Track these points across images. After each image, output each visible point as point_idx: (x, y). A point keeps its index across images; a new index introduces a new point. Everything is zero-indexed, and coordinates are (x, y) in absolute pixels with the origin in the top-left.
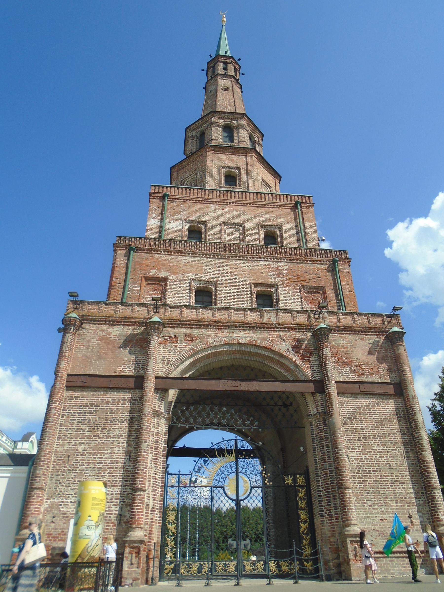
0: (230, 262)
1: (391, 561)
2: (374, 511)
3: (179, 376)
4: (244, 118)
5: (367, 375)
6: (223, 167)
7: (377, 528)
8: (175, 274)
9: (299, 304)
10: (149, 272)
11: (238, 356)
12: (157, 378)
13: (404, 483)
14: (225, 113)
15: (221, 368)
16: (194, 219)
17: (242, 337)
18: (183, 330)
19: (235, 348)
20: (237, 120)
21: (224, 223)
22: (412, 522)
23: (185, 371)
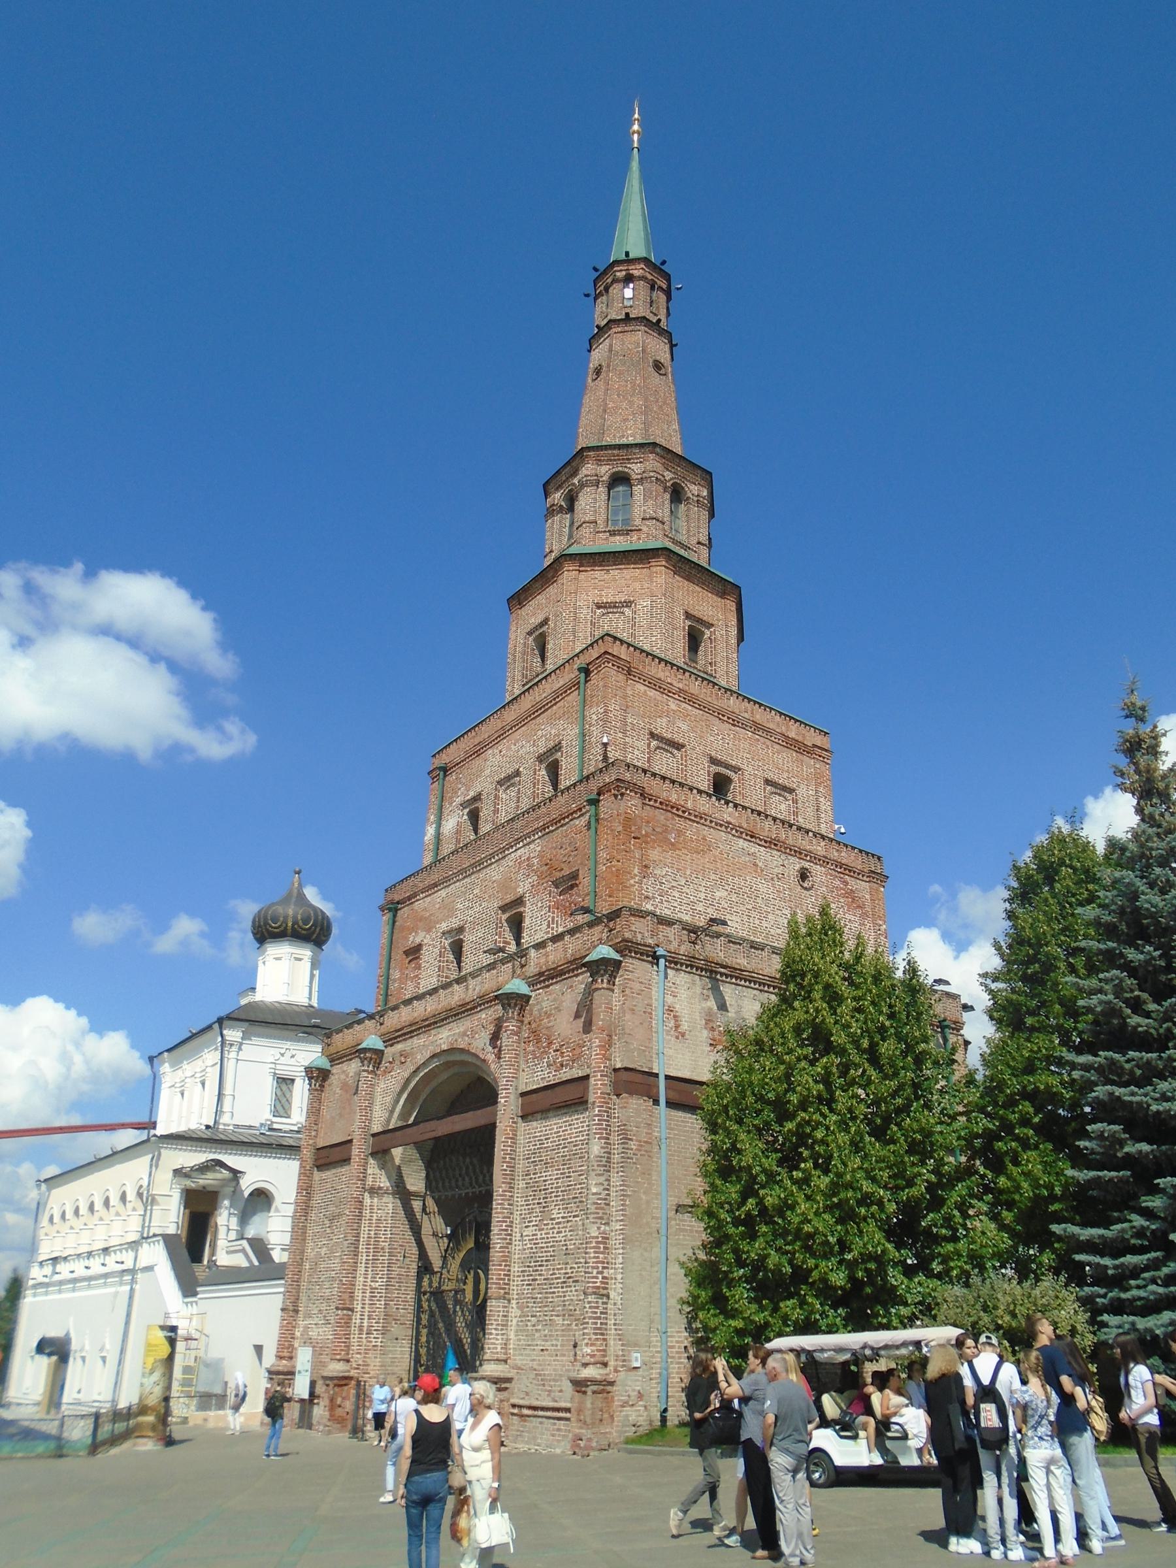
2: (537, 1335)
3: (400, 1124)
4: (587, 456)
6: (530, 633)
7: (535, 1365)
8: (429, 931)
9: (545, 926)
10: (407, 939)
11: (456, 1069)
12: (373, 1135)
13: (577, 1281)
14: (558, 472)
15: (469, 1086)
16: (472, 794)
17: (443, 1038)
18: (399, 1047)
19: (443, 1059)
20: (575, 473)
22: (575, 1355)
23: (404, 1115)
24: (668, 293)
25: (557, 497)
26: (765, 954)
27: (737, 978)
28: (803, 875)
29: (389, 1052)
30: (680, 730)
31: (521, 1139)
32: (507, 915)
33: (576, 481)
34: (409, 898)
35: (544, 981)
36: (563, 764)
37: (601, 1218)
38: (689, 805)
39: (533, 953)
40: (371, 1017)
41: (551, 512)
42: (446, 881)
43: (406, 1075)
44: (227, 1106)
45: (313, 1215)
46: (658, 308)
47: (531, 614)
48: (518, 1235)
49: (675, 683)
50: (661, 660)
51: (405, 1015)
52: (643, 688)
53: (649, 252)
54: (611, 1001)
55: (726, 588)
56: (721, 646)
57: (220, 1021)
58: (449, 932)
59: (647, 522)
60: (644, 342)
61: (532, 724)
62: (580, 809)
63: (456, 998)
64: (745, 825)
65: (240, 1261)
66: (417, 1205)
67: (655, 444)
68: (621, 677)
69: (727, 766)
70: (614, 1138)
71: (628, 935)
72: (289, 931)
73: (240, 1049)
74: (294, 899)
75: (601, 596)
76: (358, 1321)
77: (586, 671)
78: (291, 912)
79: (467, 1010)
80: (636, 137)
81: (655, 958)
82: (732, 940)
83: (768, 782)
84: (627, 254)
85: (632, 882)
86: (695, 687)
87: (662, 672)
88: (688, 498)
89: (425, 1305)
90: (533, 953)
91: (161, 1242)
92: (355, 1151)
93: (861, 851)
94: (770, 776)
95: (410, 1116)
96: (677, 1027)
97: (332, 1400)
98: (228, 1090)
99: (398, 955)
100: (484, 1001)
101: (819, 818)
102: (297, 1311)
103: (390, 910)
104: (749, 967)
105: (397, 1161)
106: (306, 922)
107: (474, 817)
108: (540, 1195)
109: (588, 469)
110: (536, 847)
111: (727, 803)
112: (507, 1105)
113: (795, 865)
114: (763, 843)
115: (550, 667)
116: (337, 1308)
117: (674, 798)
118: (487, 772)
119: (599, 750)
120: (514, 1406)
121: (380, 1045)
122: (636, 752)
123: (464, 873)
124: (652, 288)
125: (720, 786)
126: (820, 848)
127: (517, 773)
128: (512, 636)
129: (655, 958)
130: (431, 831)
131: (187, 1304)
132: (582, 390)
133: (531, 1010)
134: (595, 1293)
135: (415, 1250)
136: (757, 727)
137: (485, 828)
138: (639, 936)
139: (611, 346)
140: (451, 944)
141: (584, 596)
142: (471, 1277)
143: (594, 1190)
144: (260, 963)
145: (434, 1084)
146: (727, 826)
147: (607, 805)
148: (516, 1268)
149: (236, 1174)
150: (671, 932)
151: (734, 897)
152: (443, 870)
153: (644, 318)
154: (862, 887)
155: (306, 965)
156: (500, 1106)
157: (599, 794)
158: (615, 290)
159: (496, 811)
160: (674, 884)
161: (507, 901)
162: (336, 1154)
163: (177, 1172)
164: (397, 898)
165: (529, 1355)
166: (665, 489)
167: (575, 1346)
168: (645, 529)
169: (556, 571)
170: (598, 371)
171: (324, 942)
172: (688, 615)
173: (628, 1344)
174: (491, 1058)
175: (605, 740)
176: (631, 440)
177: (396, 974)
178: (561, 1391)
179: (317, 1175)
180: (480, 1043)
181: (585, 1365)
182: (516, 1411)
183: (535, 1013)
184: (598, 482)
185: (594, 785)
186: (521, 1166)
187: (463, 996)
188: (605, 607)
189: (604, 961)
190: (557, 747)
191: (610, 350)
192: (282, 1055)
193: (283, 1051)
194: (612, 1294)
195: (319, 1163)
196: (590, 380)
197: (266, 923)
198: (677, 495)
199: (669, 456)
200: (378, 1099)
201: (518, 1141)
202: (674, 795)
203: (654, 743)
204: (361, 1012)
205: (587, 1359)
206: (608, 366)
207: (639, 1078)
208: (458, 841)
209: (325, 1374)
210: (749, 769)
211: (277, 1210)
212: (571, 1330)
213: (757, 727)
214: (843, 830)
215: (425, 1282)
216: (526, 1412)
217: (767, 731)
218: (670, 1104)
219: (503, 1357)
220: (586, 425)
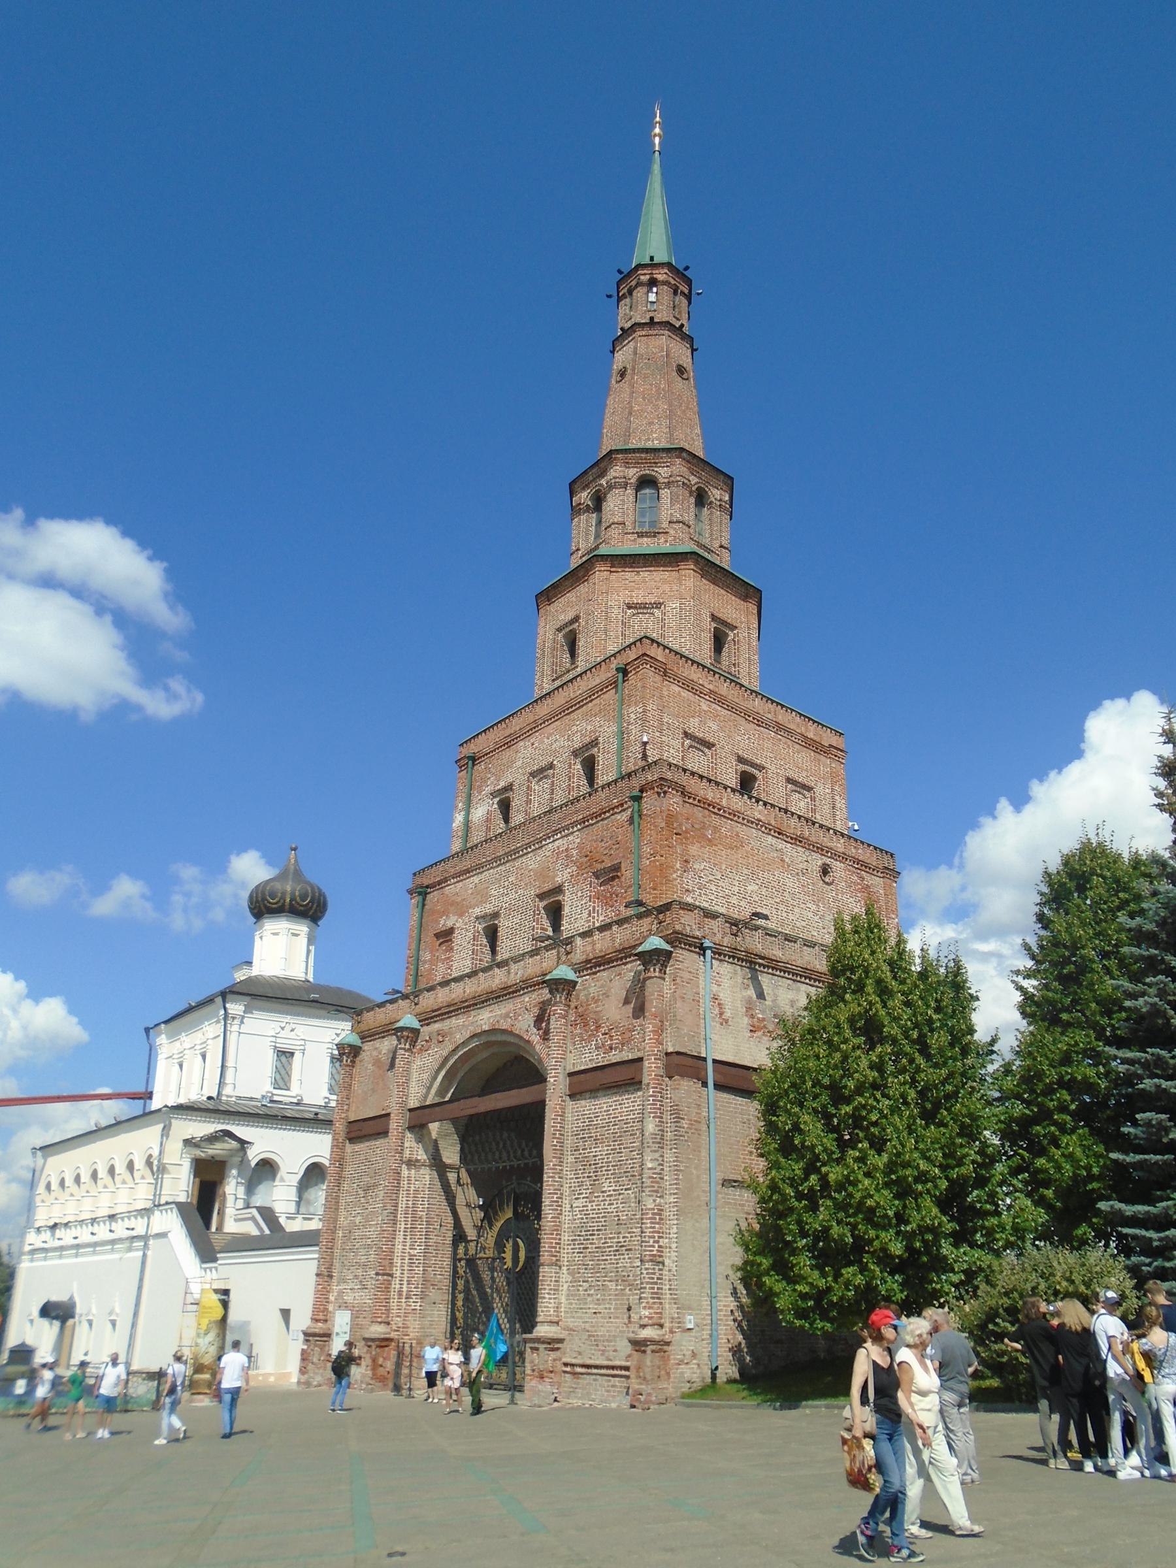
0: (517, 863)
1: (595, 1380)
2: (589, 1299)
5: (616, 1049)
6: (559, 630)
8: (461, 915)
9: (585, 915)
11: (495, 1049)
12: (410, 1110)
14: (585, 472)
16: (502, 784)
17: (484, 1018)
18: (437, 1026)
19: (483, 1039)
20: (602, 474)
21: (531, 774)
23: (442, 1091)
24: (689, 297)
25: (584, 497)
26: (797, 946)
27: (773, 968)
28: (825, 870)
29: (425, 1031)
30: (710, 729)
31: (569, 1116)
32: (545, 903)
33: (603, 482)
34: (439, 883)
35: (591, 968)
36: (600, 759)
37: (657, 1191)
38: (724, 803)
39: (579, 941)
40: (405, 997)
41: (576, 511)
42: (479, 868)
43: (445, 1054)
44: (229, 1078)
45: (345, 1186)
46: (680, 312)
47: (562, 610)
48: (568, 1206)
49: (706, 685)
50: (693, 662)
51: (442, 996)
52: (677, 689)
53: (670, 256)
54: (660, 989)
55: (749, 593)
56: (744, 647)
57: (224, 995)
58: (483, 917)
59: (674, 526)
60: (668, 346)
61: (566, 720)
62: (622, 805)
63: (497, 981)
64: (773, 823)
65: (250, 1229)
66: (452, 1177)
67: (682, 450)
68: (658, 678)
69: (753, 765)
70: (667, 1117)
71: (678, 927)
72: (287, 907)
73: (242, 1022)
74: (291, 877)
75: (632, 597)
76: (398, 1286)
77: (624, 671)
78: (289, 889)
79: (509, 993)
80: (657, 140)
81: (703, 950)
82: (769, 933)
83: (789, 780)
84: (652, 258)
86: (724, 688)
87: (695, 674)
88: (711, 503)
89: (461, 1272)
90: (579, 941)
91: (175, 1210)
92: (393, 1125)
93: (876, 848)
94: (791, 774)
95: (447, 1092)
96: (721, 1014)
97: (374, 1360)
98: (230, 1063)
99: (428, 937)
100: (528, 985)
101: (834, 815)
102: (331, 1277)
103: (420, 893)
104: (784, 959)
105: (434, 1135)
106: (303, 898)
107: (505, 807)
108: (591, 1171)
109: (616, 471)
110: (575, 839)
111: (750, 798)
112: (556, 1085)
113: (818, 860)
115: (582, 665)
116: (377, 1274)
117: (710, 796)
118: (519, 763)
119: (638, 748)
120: (566, 1365)
121: (416, 1024)
122: (672, 751)
123: (498, 860)
124: (675, 293)
125: (746, 783)
126: (839, 845)
127: (551, 766)
128: (541, 631)
129: (703, 950)
130: (459, 818)
131: (205, 1269)
132: (607, 390)
133: (578, 995)
134: (651, 1261)
135: (450, 1220)
136: (779, 728)
137: (517, 818)
138: (688, 928)
139: (635, 348)
140: (484, 929)
141: (615, 596)
142: (509, 1247)
143: (650, 1165)
144: (257, 938)
145: (473, 1061)
146: (757, 823)
147: (650, 802)
148: (565, 1237)
149: (243, 1143)
150: (715, 925)
152: (472, 858)
153: (668, 322)
155: (303, 941)
156: (549, 1086)
157: (641, 791)
158: (639, 293)
159: (529, 802)
160: (711, 878)
161: (545, 889)
162: (369, 1128)
163: (188, 1142)
164: (426, 882)
165: (581, 1318)
166: (691, 492)
167: (629, 1309)
168: (672, 532)
169: (588, 571)
170: (622, 374)
171: (320, 918)
172: (714, 618)
173: (684, 1307)
174: (535, 1037)
175: (645, 739)
176: (656, 444)
177: (426, 956)
178: (615, 1351)
179: (349, 1148)
180: (525, 1025)
181: (643, 1326)
182: (568, 1369)
183: (582, 997)
184: (626, 484)
185: (636, 782)
186: (569, 1142)
187: (504, 979)
188: (636, 608)
189: (657, 952)
190: (594, 743)
191: (635, 353)
192: (283, 1028)
193: (283, 1025)
194: (667, 1262)
195: (353, 1135)
196: (613, 382)
197: (264, 899)
198: (701, 499)
200: (415, 1076)
201: (566, 1119)
202: (710, 794)
203: (688, 742)
204: (398, 992)
205: (645, 1321)
206: (633, 369)
207: (690, 1061)
208: (488, 829)
209: (367, 1336)
210: (772, 768)
211: (282, 1180)
212: (623, 1295)
213: (779, 728)
214: (856, 827)
215: (461, 1250)
216: (579, 1370)
217: (788, 731)
218: (718, 1087)
219: (556, 1319)
220: (611, 426)
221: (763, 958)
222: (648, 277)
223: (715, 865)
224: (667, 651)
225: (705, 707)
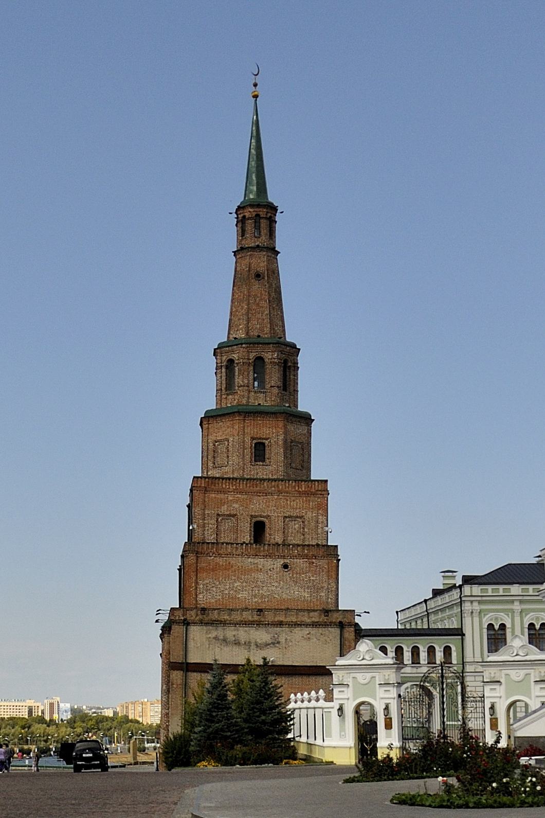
28: (285, 566)
52: (213, 495)
75: (216, 436)
85: (191, 589)
101: (318, 526)
104: (230, 619)
114: (262, 557)
122: (210, 526)
136: (280, 492)
138: (177, 618)
146: (242, 555)
150: (193, 613)
151: (244, 584)
154: (323, 563)
160: (213, 585)
199: (251, 345)
210: (273, 515)
221: (217, 621)
222: (242, 215)
223: (215, 579)
224: (207, 480)
225: (230, 498)
